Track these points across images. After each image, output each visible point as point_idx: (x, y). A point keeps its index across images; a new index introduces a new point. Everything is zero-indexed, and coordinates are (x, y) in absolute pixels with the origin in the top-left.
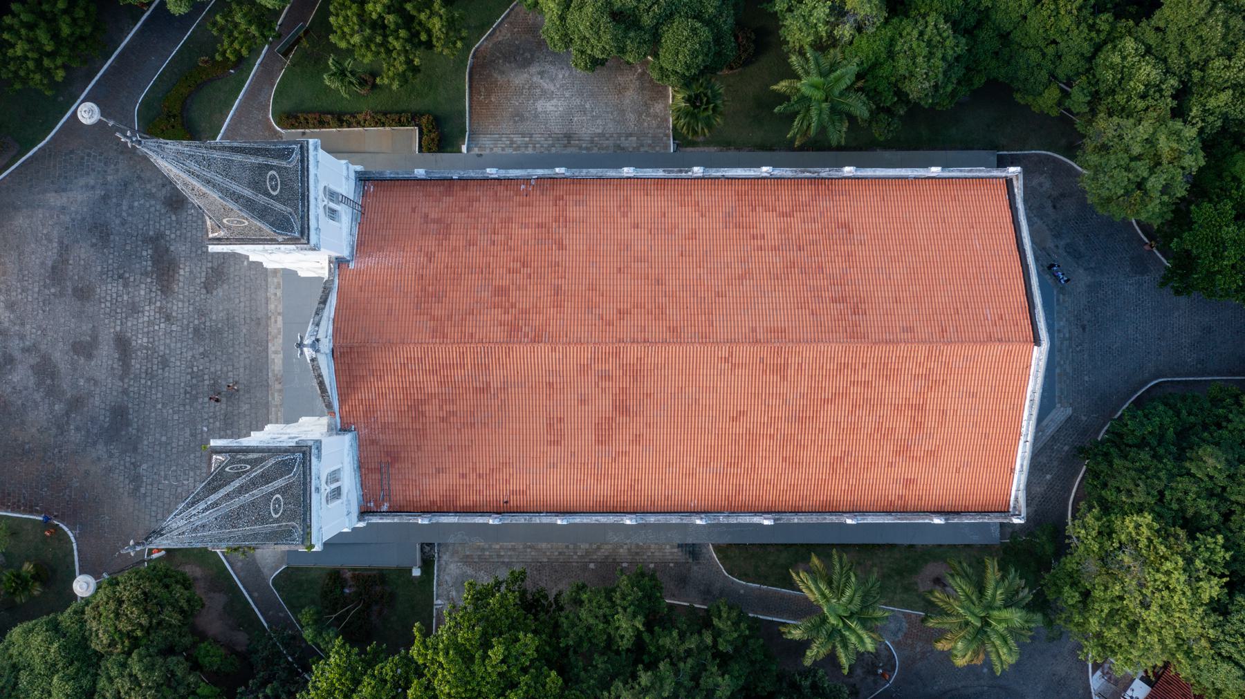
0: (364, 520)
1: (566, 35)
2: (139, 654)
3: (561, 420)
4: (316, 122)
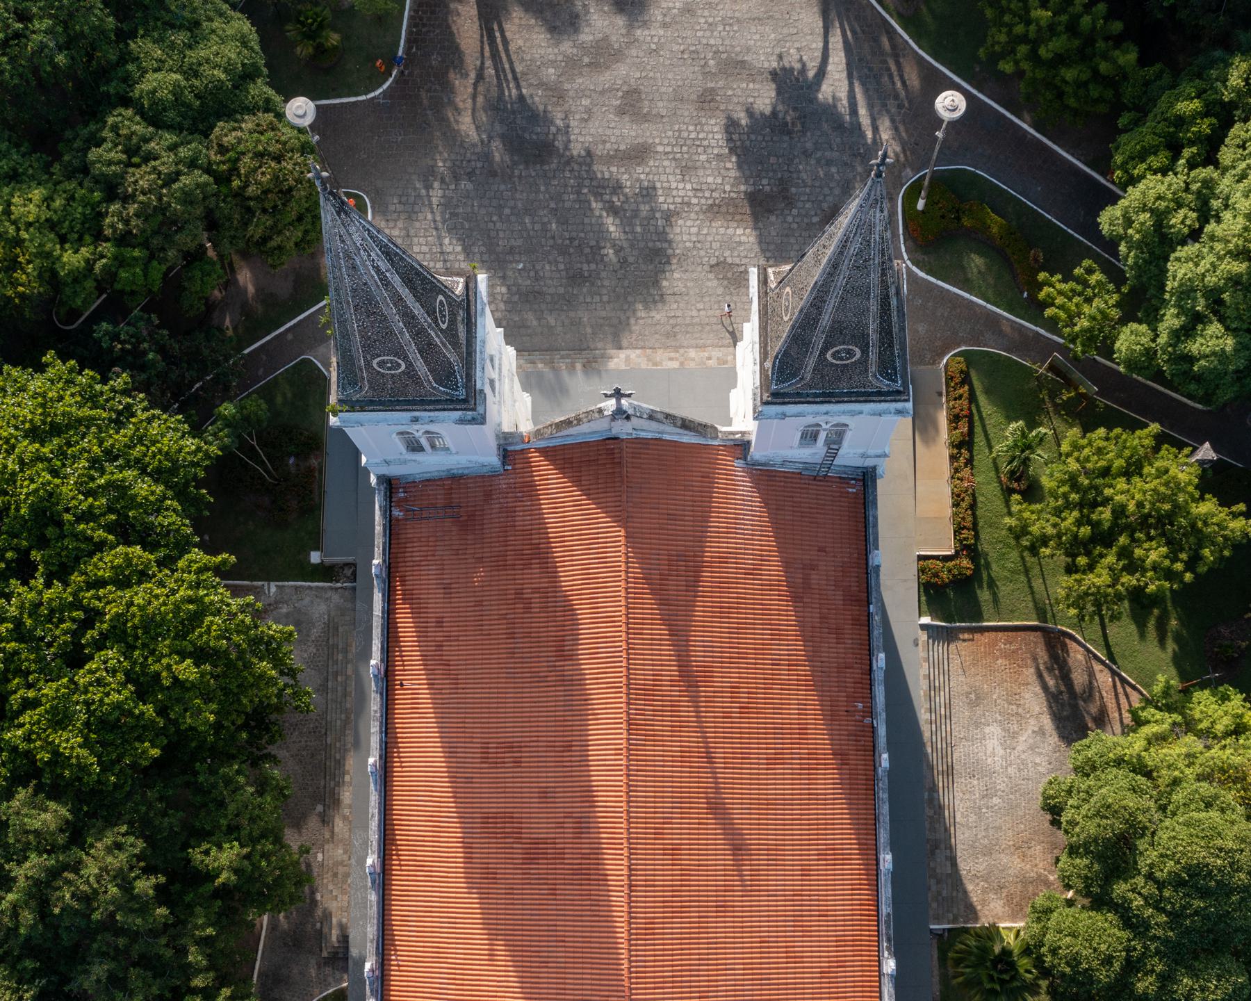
0: (378, 484)
1: (1094, 768)
2: (206, 184)
3: (518, 762)
4: (957, 411)
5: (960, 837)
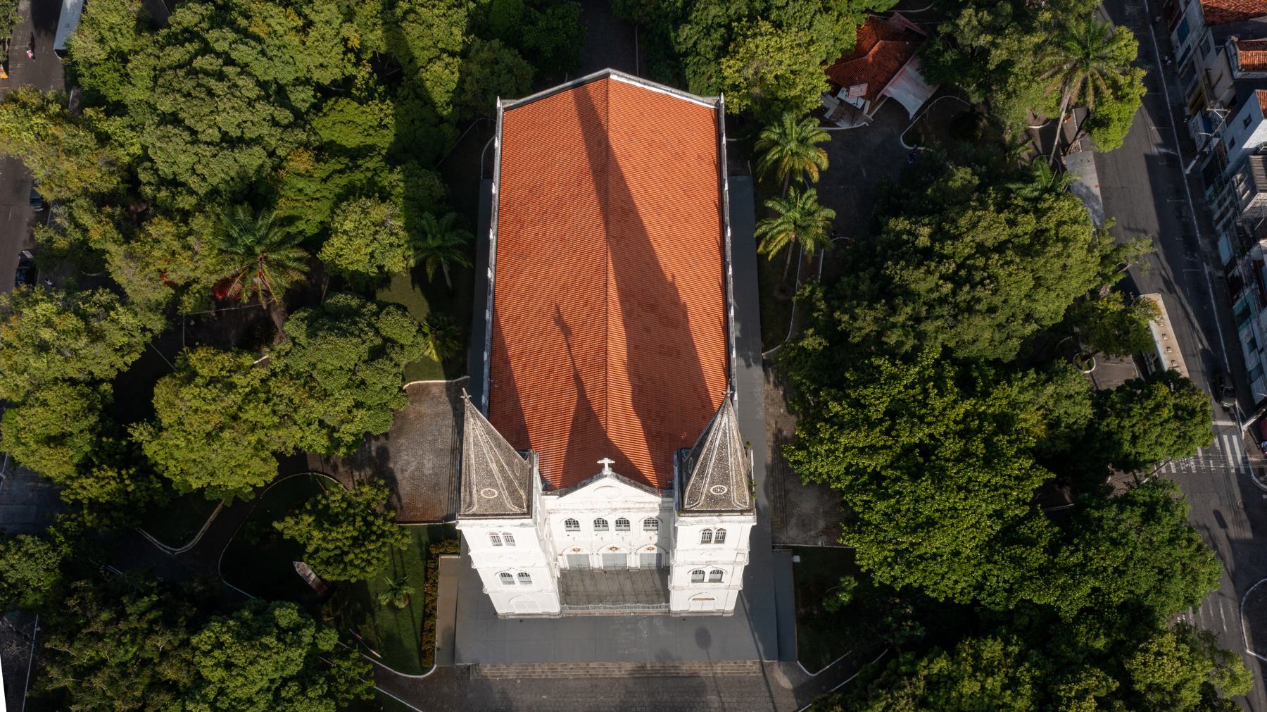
5: (450, 421)
